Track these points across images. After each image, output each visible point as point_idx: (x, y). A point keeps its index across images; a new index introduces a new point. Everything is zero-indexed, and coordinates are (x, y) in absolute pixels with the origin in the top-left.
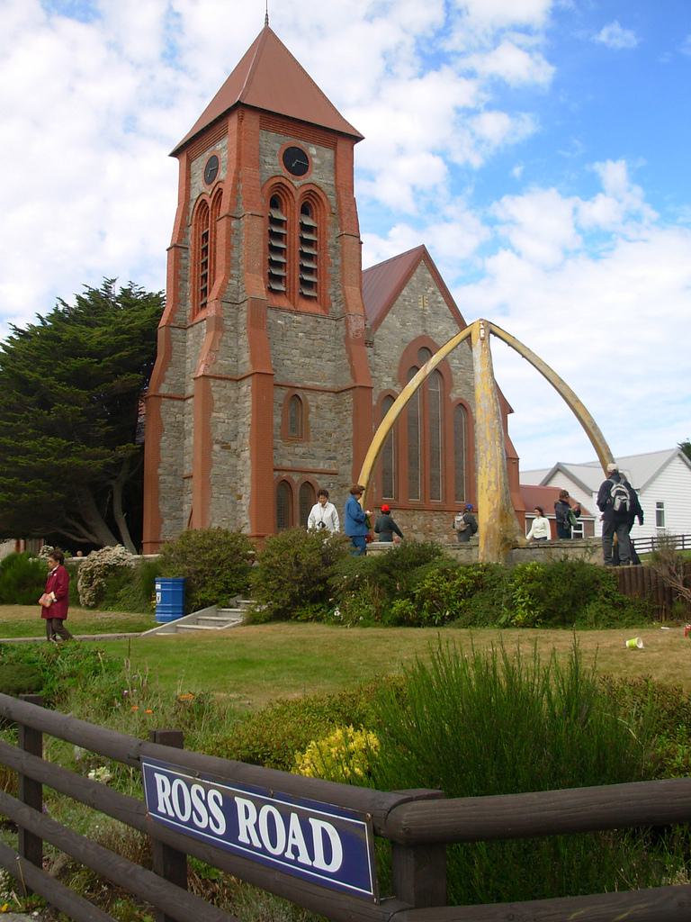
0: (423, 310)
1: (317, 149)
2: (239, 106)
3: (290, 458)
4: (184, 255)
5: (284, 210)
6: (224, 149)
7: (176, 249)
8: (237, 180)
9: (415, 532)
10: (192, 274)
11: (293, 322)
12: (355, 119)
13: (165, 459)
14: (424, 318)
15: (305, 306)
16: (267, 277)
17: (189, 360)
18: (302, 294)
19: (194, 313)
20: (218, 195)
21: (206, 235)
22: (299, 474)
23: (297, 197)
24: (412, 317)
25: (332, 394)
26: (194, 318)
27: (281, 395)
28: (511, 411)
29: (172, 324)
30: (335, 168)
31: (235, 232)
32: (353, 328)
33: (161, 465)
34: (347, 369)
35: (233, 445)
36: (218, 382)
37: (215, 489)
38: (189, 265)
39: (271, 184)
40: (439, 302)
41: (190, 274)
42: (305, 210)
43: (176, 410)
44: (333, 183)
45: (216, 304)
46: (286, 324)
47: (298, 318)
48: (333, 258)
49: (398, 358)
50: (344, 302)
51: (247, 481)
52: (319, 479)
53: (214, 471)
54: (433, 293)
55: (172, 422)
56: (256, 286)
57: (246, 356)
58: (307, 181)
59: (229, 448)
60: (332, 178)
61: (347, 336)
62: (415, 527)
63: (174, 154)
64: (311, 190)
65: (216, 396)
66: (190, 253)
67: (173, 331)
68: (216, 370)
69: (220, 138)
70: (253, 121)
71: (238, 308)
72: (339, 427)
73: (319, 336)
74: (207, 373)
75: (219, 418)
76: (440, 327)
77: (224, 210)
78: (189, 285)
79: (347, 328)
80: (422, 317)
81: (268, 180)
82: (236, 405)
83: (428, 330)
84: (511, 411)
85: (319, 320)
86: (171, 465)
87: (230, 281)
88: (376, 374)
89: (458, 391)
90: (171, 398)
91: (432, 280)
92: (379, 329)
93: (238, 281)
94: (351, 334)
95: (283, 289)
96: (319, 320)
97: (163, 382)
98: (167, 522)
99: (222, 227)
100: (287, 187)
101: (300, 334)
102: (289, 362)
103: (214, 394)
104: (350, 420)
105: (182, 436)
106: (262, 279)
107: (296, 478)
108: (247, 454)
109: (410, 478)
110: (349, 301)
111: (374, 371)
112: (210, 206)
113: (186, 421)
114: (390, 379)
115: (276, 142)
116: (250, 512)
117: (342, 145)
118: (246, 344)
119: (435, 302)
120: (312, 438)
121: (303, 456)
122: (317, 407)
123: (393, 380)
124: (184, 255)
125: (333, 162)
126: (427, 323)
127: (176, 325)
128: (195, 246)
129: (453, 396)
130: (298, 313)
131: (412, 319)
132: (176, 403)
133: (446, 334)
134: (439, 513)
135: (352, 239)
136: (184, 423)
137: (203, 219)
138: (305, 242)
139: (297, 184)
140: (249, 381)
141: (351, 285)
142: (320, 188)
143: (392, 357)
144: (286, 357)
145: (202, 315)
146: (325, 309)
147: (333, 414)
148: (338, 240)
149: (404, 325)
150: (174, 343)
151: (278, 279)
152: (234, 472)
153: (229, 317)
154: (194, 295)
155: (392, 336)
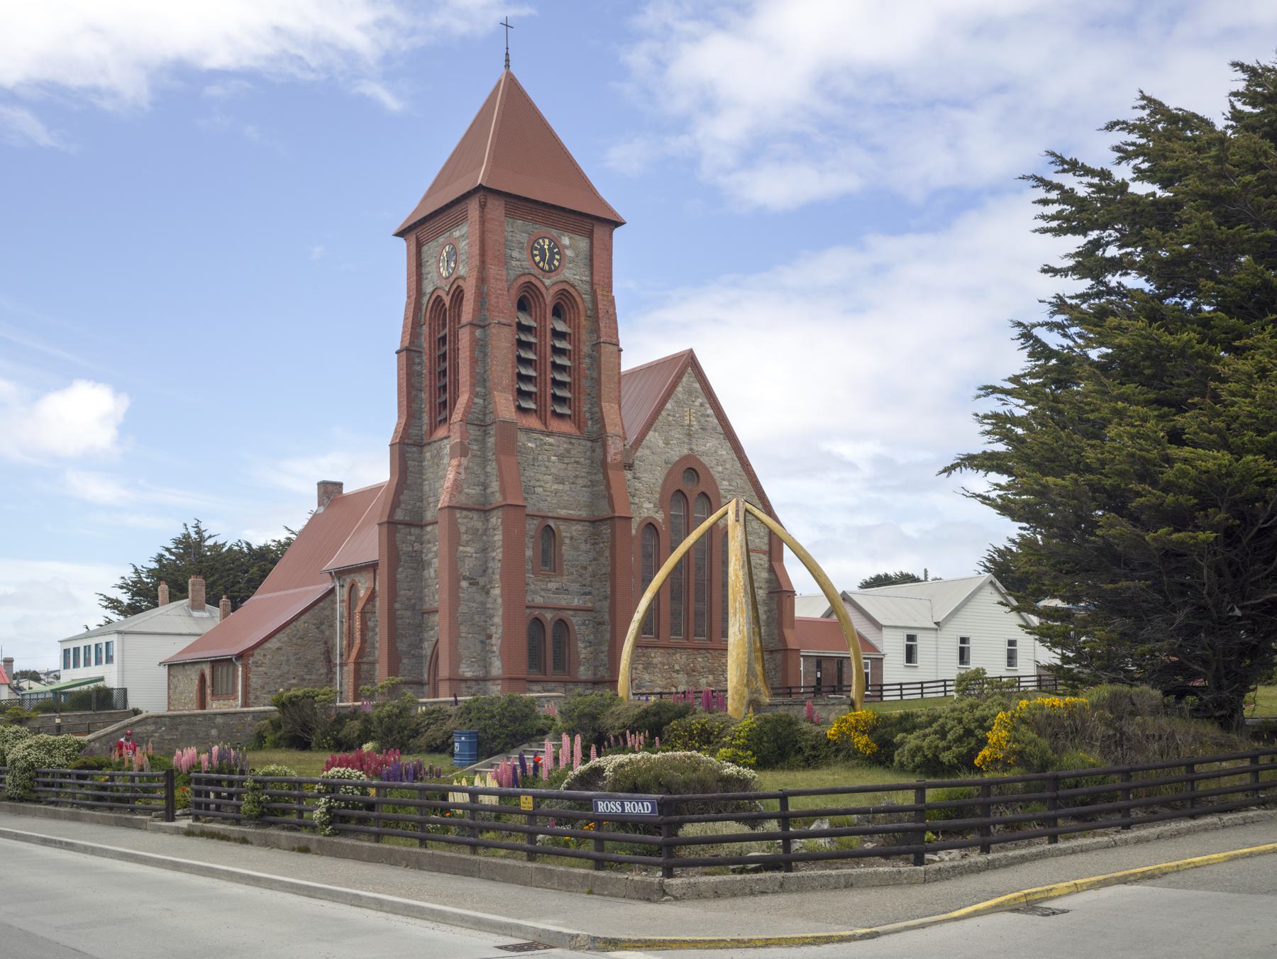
0: (690, 425)
2: (481, 188)
4: (417, 360)
5: (533, 314)
6: (464, 236)
7: (409, 353)
8: (482, 280)
9: (677, 672)
10: (428, 383)
11: (545, 444)
12: (614, 198)
13: (402, 593)
14: (690, 435)
15: (555, 425)
16: (515, 394)
17: (427, 482)
18: (554, 412)
19: (431, 428)
20: (458, 295)
21: (444, 339)
22: (553, 611)
23: (549, 299)
24: (676, 433)
25: (587, 524)
26: (431, 434)
27: (532, 526)
29: (406, 441)
30: (591, 260)
32: (612, 450)
33: (398, 599)
34: (604, 497)
35: (482, 581)
36: (465, 513)
37: (463, 629)
38: (424, 371)
39: (522, 282)
40: (708, 416)
41: (426, 382)
43: (413, 538)
45: (461, 426)
46: (537, 446)
47: (550, 440)
48: (588, 369)
49: (660, 481)
50: (600, 420)
51: (497, 620)
52: (572, 616)
53: (463, 608)
54: (702, 405)
55: (409, 552)
56: (505, 406)
57: (495, 486)
59: (477, 584)
60: (587, 273)
61: (604, 461)
62: (677, 667)
63: (401, 234)
64: (564, 290)
65: (463, 529)
66: (425, 358)
67: (408, 449)
68: (462, 500)
69: (457, 224)
70: (496, 208)
71: (485, 431)
72: (595, 559)
73: (572, 460)
74: (454, 503)
75: (466, 552)
77: (467, 313)
78: (425, 396)
79: (605, 452)
80: (690, 435)
82: (485, 538)
83: (694, 447)
85: (573, 441)
86: (409, 599)
87: (476, 400)
88: (636, 500)
90: (408, 525)
91: (700, 391)
93: (485, 400)
94: (609, 460)
95: (533, 406)
96: (573, 441)
97: (399, 507)
98: (405, 661)
99: (465, 337)
101: (553, 458)
102: (541, 489)
103: (459, 526)
104: (607, 553)
105: (420, 567)
106: (511, 398)
107: (549, 616)
108: (497, 591)
109: (672, 614)
110: (607, 421)
111: (634, 496)
112: (447, 305)
113: (425, 551)
114: (651, 506)
115: (523, 232)
116: (501, 653)
117: (599, 231)
118: (495, 472)
119: (703, 415)
120: (566, 572)
121: (557, 591)
122: (571, 538)
124: (417, 360)
125: (589, 253)
127: (410, 442)
128: (430, 351)
130: (550, 434)
132: (413, 530)
134: (703, 651)
135: (611, 347)
136: (422, 552)
137: (439, 319)
138: (557, 351)
140: (499, 513)
141: (608, 402)
143: (654, 481)
144: (538, 484)
145: (441, 432)
146: (579, 428)
147: (588, 546)
149: (667, 444)
150: (409, 462)
151: (528, 395)
152: (485, 612)
153: (475, 440)
154: (431, 408)
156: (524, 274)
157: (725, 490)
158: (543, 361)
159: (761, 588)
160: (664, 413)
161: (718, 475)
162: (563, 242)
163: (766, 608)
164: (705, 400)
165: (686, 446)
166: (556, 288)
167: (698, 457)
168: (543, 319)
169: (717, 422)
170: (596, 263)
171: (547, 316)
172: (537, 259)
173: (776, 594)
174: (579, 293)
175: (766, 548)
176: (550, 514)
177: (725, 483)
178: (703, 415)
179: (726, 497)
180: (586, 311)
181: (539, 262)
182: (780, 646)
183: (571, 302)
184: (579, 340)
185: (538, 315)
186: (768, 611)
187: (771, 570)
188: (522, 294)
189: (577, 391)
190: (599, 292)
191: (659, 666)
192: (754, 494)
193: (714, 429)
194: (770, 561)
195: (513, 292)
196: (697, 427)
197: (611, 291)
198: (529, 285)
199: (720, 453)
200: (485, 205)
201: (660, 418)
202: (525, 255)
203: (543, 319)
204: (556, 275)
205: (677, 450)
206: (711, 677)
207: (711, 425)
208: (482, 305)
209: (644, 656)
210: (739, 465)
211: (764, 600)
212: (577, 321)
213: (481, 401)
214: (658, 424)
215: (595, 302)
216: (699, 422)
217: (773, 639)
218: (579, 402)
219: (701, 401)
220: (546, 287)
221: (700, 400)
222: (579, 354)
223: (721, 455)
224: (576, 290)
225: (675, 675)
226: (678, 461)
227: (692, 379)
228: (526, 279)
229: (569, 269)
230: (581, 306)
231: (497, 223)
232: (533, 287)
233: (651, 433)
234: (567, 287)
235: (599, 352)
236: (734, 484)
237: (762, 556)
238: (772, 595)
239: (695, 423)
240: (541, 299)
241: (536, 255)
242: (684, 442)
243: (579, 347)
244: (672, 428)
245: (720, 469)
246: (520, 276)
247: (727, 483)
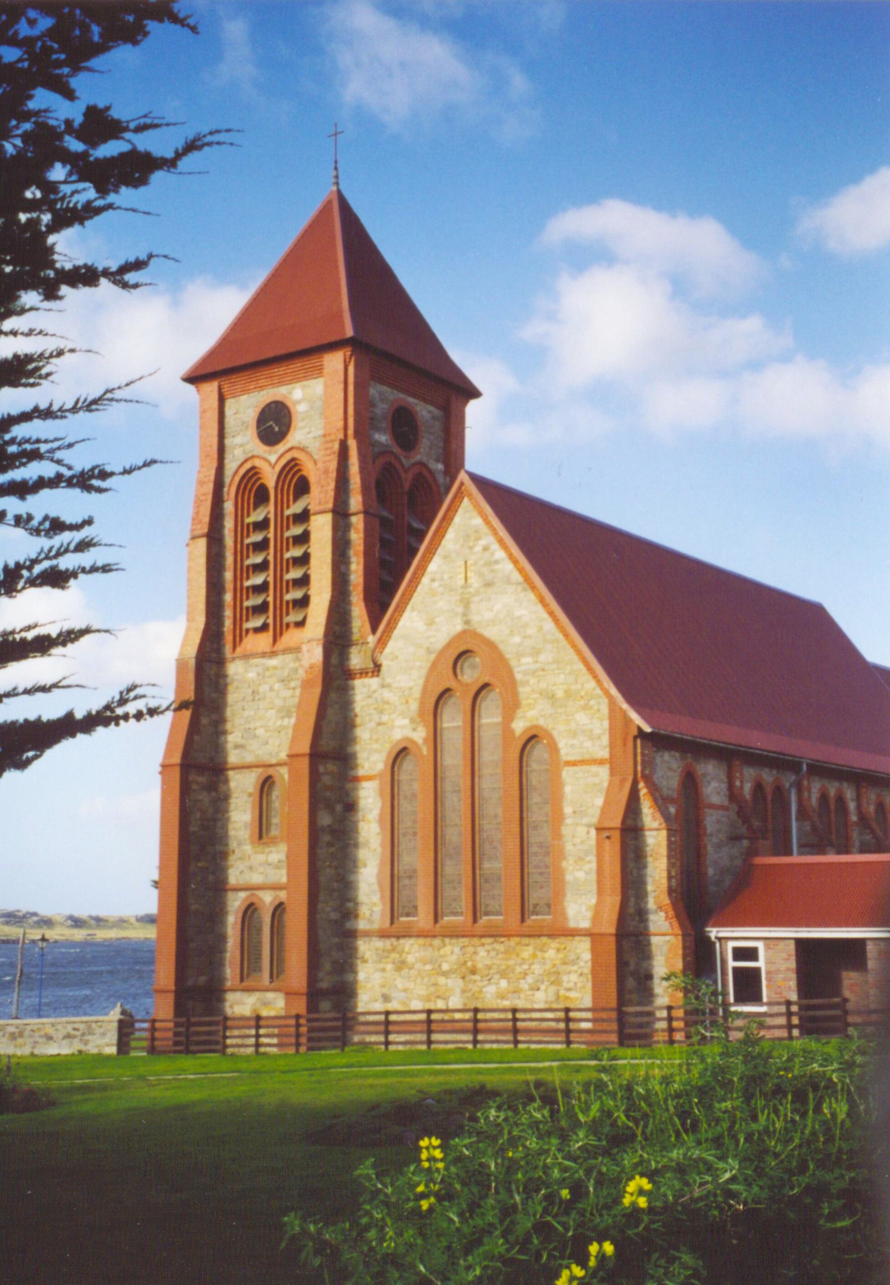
3: (261, 870)
9: (445, 974)
11: (268, 669)
40: (497, 562)
49: (421, 682)
54: (486, 549)
58: (288, 446)
62: (445, 967)
88: (385, 718)
111: (381, 712)
123: (412, 721)
149: (430, 623)
157: (525, 673)
160: (425, 580)
176: (274, 761)
191: (418, 966)
199: (517, 613)
206: (504, 983)
209: (394, 949)
221: (483, 542)
225: (442, 980)
247: (529, 660)
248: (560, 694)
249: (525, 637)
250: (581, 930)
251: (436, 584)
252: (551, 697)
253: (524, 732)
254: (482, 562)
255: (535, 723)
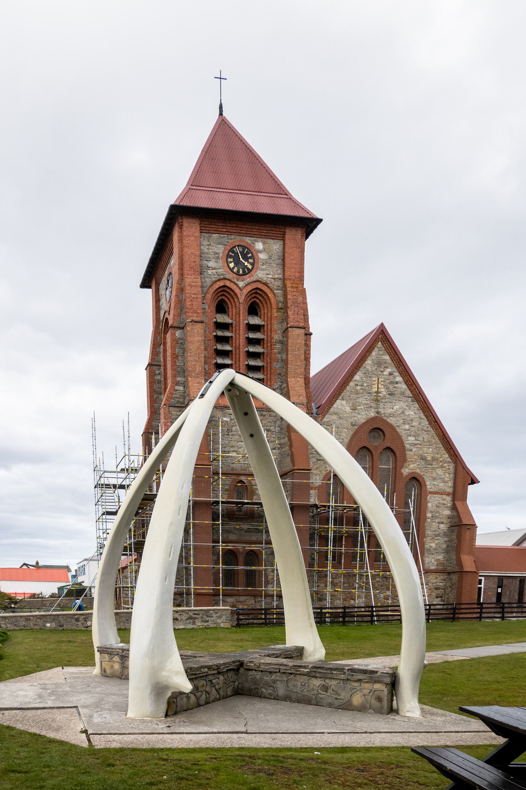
1: (264, 243)
5: (230, 314)
14: (377, 400)
23: (242, 296)
24: (363, 400)
28: (474, 481)
30: (283, 260)
31: (181, 341)
39: (217, 287)
40: (397, 383)
42: (253, 310)
44: (281, 276)
48: (279, 353)
54: (390, 374)
64: (257, 288)
76: (395, 408)
80: (377, 400)
81: (211, 286)
83: (381, 410)
84: (474, 481)
89: (412, 466)
91: (390, 361)
92: (327, 416)
93: (184, 387)
100: (230, 289)
119: (391, 383)
125: (282, 254)
126: (381, 405)
129: (405, 471)
131: (363, 402)
133: (403, 413)
138: (251, 342)
139: (241, 284)
142: (266, 284)
148: (284, 335)
149: (354, 409)
155: (341, 421)
156: (219, 280)
157: (411, 444)
158: (237, 351)
159: (442, 523)
160: (352, 384)
161: (404, 432)
162: (257, 248)
163: (446, 539)
164: (395, 369)
165: (373, 409)
166: (249, 288)
167: (385, 418)
168: (237, 316)
169: (406, 387)
170: (287, 260)
171: (241, 312)
172: (232, 265)
173: (456, 528)
174: (271, 289)
175: (450, 490)
177: (412, 438)
178: (391, 383)
179: (411, 450)
180: (278, 304)
181: (234, 268)
182: (457, 569)
183: (260, 295)
184: (271, 330)
185: (234, 312)
186: (449, 541)
187: (454, 508)
188: (220, 298)
189: (269, 372)
190: (289, 284)
192: (441, 446)
193: (403, 393)
194: (453, 500)
195: (209, 296)
196: (385, 393)
197: (303, 284)
198: (225, 289)
200: (182, 225)
201: (348, 388)
202: (221, 263)
203: (237, 316)
204: (249, 277)
205: (363, 413)
207: (399, 390)
208: (181, 310)
210: (427, 423)
211: (445, 532)
212: (269, 314)
213: (181, 388)
214: (346, 393)
215: (285, 295)
216: (388, 388)
217: (451, 563)
218: (271, 382)
219: (390, 370)
220: (240, 288)
221: (389, 370)
222: (271, 342)
223: (409, 415)
224: (269, 287)
226: (365, 423)
227: (381, 353)
228: (221, 284)
229: (263, 270)
230: (273, 300)
231: (193, 238)
232: (228, 290)
233: (338, 402)
234: (260, 286)
235: (287, 338)
236: (421, 438)
237: (445, 497)
238: (451, 528)
239: (383, 390)
240: (236, 300)
241: (231, 262)
242: (371, 407)
243: (271, 336)
244: (360, 396)
245: (407, 427)
246: (216, 282)
247: (413, 438)
248: (429, 458)
249: (411, 426)
250: (432, 570)
251: (359, 388)
252: (423, 458)
253: (408, 475)
254: (388, 381)
255: (414, 471)
